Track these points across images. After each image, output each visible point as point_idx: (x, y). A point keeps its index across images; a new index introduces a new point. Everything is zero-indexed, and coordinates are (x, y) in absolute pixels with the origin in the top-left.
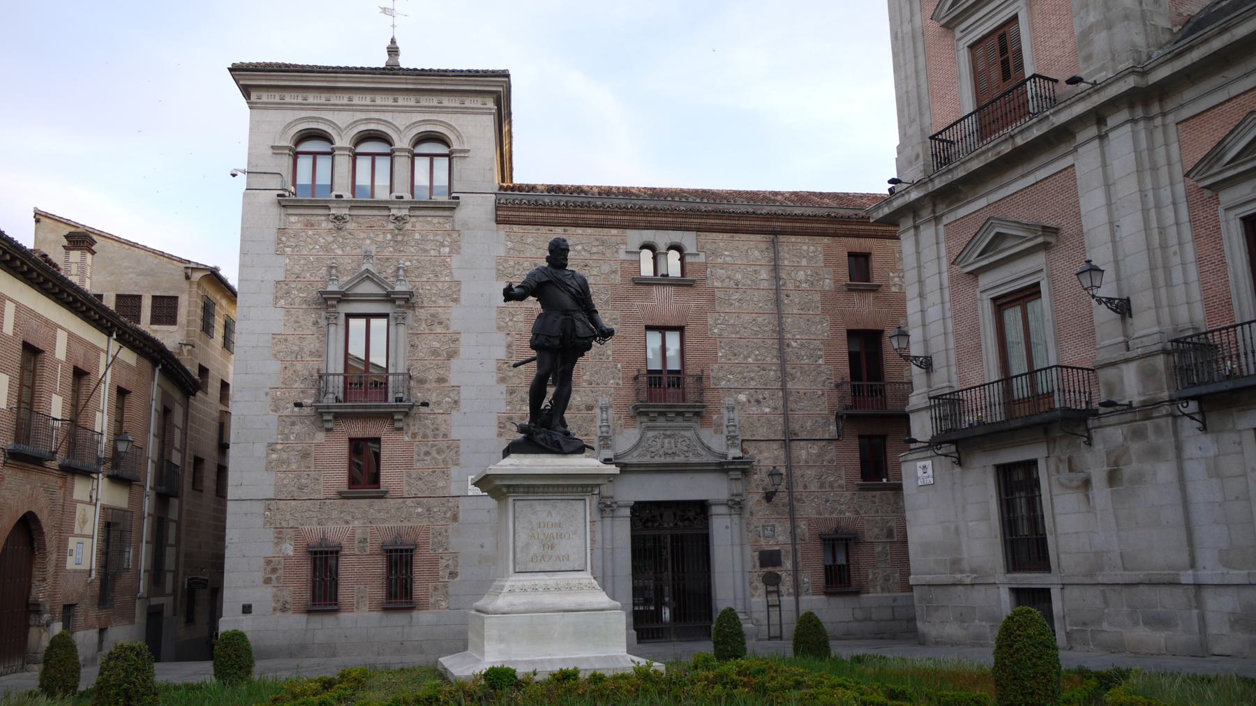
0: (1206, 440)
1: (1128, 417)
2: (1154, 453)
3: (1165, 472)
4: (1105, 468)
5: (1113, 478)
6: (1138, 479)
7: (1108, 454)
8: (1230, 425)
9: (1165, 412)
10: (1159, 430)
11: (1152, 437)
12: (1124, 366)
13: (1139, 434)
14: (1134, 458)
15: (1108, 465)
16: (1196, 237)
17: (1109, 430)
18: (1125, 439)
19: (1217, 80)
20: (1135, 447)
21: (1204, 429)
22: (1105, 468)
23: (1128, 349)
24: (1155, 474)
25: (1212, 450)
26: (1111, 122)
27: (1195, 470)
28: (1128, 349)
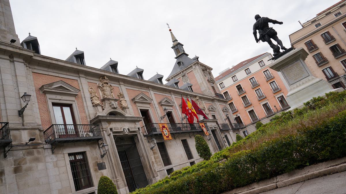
0: (53, 156)
1: (27, 147)
2: (37, 160)
3: (41, 166)
4: (13, 166)
5: (17, 170)
6: (30, 169)
7: (15, 161)
8: (60, 152)
9: (42, 147)
10: (39, 152)
11: (36, 155)
12: (22, 131)
13: (30, 154)
14: (28, 162)
15: (14, 165)
16: (38, 102)
17: (15, 153)
18: (24, 155)
19: (46, 69)
20: (28, 158)
21: (53, 153)
22: (13, 166)
23: (23, 125)
24: (37, 167)
25: (55, 160)
26: (15, 59)
27: (50, 166)
28: (23, 125)
